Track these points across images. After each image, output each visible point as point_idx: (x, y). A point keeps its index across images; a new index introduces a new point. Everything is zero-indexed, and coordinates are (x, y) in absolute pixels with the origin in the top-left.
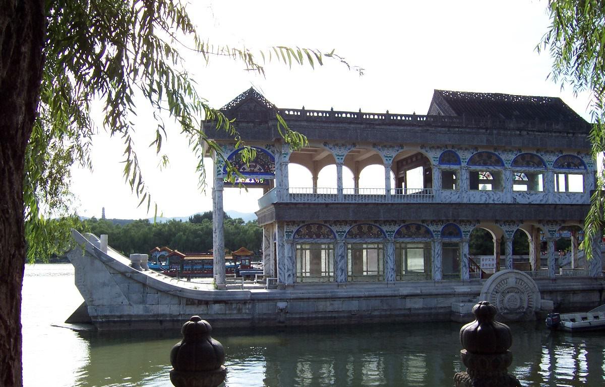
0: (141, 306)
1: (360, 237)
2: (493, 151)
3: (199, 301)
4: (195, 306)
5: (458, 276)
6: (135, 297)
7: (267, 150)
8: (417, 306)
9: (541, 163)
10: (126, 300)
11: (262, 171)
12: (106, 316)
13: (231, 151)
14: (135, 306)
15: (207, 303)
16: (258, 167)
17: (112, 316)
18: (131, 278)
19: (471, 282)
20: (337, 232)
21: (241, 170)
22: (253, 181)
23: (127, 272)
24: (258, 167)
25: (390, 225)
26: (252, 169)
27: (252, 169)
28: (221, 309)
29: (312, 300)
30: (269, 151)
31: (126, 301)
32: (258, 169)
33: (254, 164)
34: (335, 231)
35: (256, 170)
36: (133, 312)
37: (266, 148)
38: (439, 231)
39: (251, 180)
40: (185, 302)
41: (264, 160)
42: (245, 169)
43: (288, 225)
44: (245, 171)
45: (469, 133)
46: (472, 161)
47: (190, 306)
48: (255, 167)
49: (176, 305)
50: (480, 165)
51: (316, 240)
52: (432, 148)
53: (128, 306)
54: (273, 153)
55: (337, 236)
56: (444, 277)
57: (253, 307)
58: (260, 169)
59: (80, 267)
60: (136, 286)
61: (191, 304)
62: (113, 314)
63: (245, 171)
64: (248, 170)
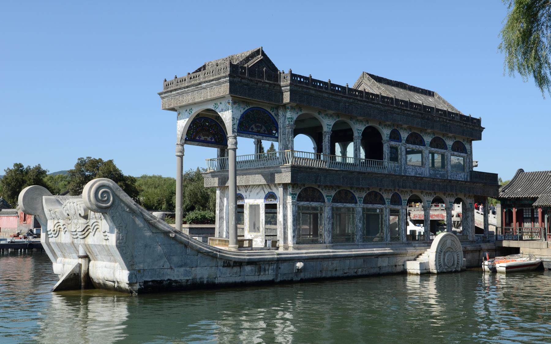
0: (182, 270)
1: (340, 202)
2: (419, 133)
3: (235, 262)
4: (231, 268)
5: (398, 239)
6: (175, 259)
7: (271, 112)
8: (384, 265)
9: (444, 147)
10: (168, 263)
11: (266, 132)
12: (146, 282)
14: (176, 270)
15: (239, 264)
16: (264, 128)
17: (152, 281)
18: (174, 238)
19: (408, 244)
20: (327, 196)
21: (250, 130)
22: (213, 140)
23: (170, 232)
24: (264, 128)
25: (360, 191)
26: (259, 129)
27: (259, 129)
28: (252, 270)
29: (320, 260)
30: (273, 114)
31: (167, 265)
33: (260, 125)
34: (324, 195)
35: (262, 131)
36: (174, 277)
38: (389, 199)
39: (211, 139)
40: (222, 264)
43: (293, 187)
45: (412, 116)
46: (408, 141)
47: (225, 268)
49: (214, 268)
50: (411, 144)
51: (311, 203)
52: (386, 126)
53: (169, 270)
55: (326, 200)
56: (392, 239)
57: (278, 268)
58: (264, 131)
59: (121, 225)
60: (178, 246)
61: (226, 266)
62: (154, 279)
64: (255, 130)
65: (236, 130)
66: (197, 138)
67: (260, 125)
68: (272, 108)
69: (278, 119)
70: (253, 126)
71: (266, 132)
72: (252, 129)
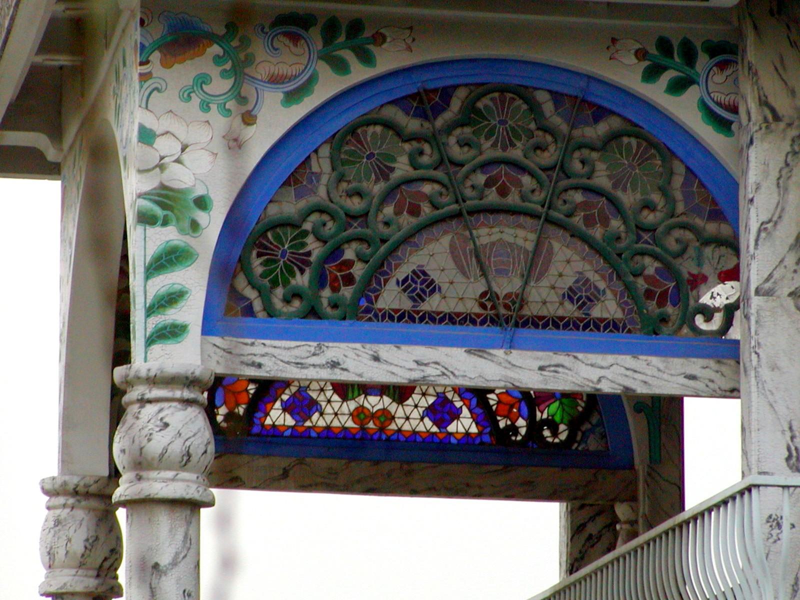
7: (656, 92)
11: (608, 308)
13: (292, 97)
21: (391, 297)
22: (464, 424)
24: (568, 263)
26: (507, 285)
32: (570, 295)
35: (543, 297)
37: (652, 73)
39: (442, 411)
41: (628, 199)
42: (432, 288)
44: (433, 304)
48: (535, 264)
54: (724, 125)
63: (433, 304)
64: (459, 292)
65: (191, 312)
67: (520, 236)
68: (671, 57)
69: (741, 153)
70: (435, 256)
71: (608, 308)
72: (421, 285)
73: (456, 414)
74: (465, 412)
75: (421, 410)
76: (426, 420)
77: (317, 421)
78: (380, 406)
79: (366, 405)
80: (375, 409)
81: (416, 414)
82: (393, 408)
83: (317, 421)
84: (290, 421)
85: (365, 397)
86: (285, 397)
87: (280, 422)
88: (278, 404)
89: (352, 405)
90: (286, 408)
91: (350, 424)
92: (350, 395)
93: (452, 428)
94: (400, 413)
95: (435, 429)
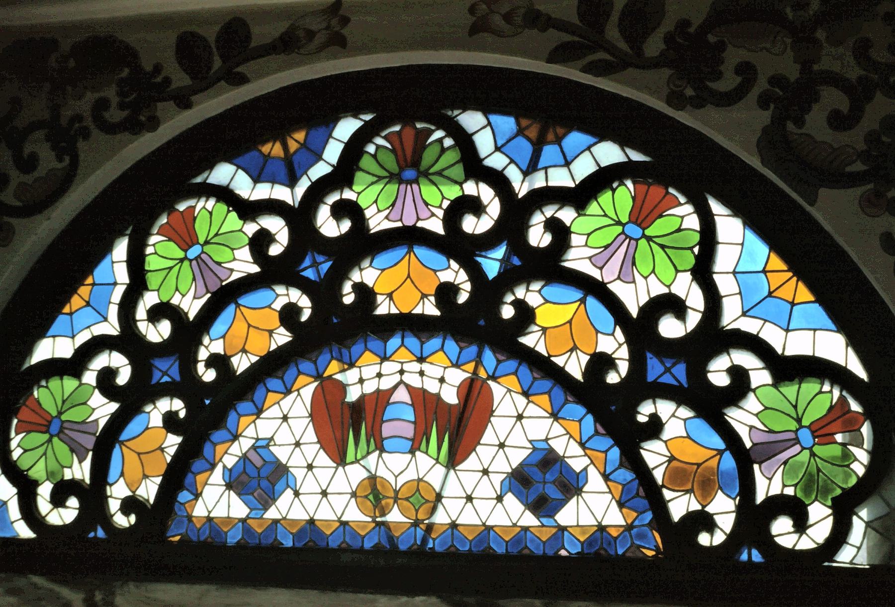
66: (215, 501)
73: (572, 486)
74: (595, 481)
75: (497, 479)
76: (510, 498)
77: (287, 508)
78: (411, 475)
79: (382, 472)
80: (401, 481)
81: (486, 489)
82: (435, 476)
83: (287, 508)
84: (238, 509)
85: (380, 455)
86: (230, 461)
87: (219, 512)
88: (217, 476)
89: (356, 474)
90: (236, 482)
91: (354, 514)
92: (350, 456)
93: (566, 516)
94: (452, 489)
95: (529, 520)
